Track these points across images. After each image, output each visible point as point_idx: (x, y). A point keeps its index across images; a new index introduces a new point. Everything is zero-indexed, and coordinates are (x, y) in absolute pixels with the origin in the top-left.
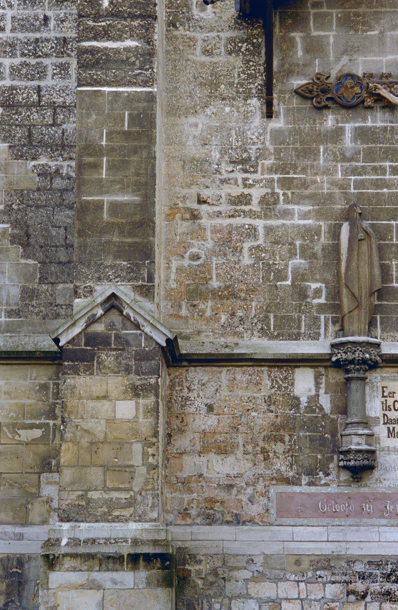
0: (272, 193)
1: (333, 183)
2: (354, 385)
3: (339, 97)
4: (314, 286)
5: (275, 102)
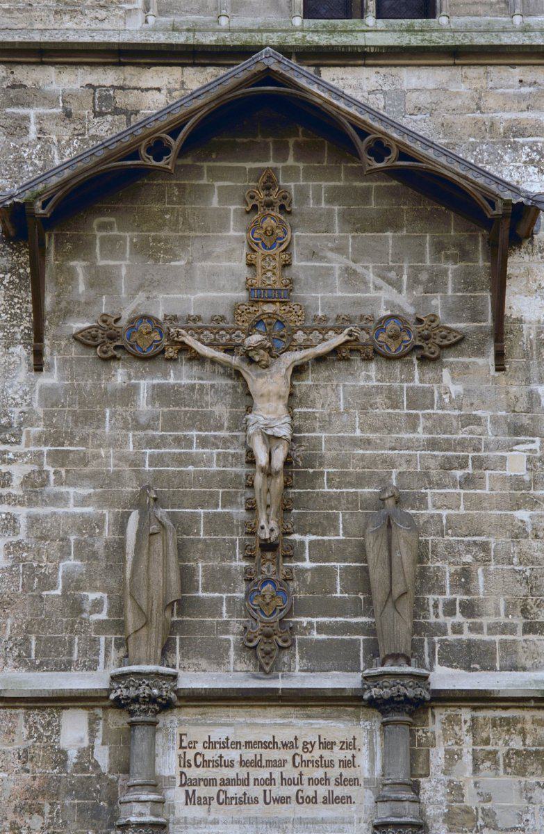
0: (39, 471)
1: (122, 458)
2: (139, 733)
3: (132, 346)
4: (93, 596)
5: (47, 350)
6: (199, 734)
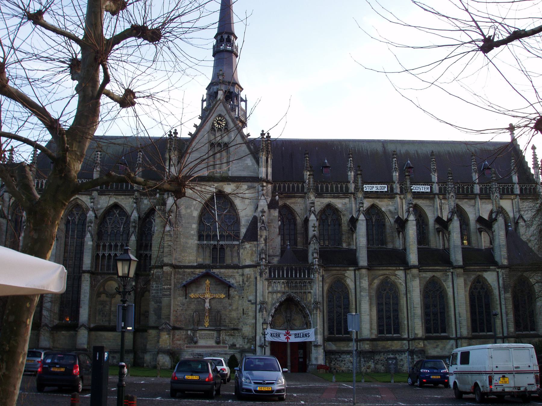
6: (200, 333)
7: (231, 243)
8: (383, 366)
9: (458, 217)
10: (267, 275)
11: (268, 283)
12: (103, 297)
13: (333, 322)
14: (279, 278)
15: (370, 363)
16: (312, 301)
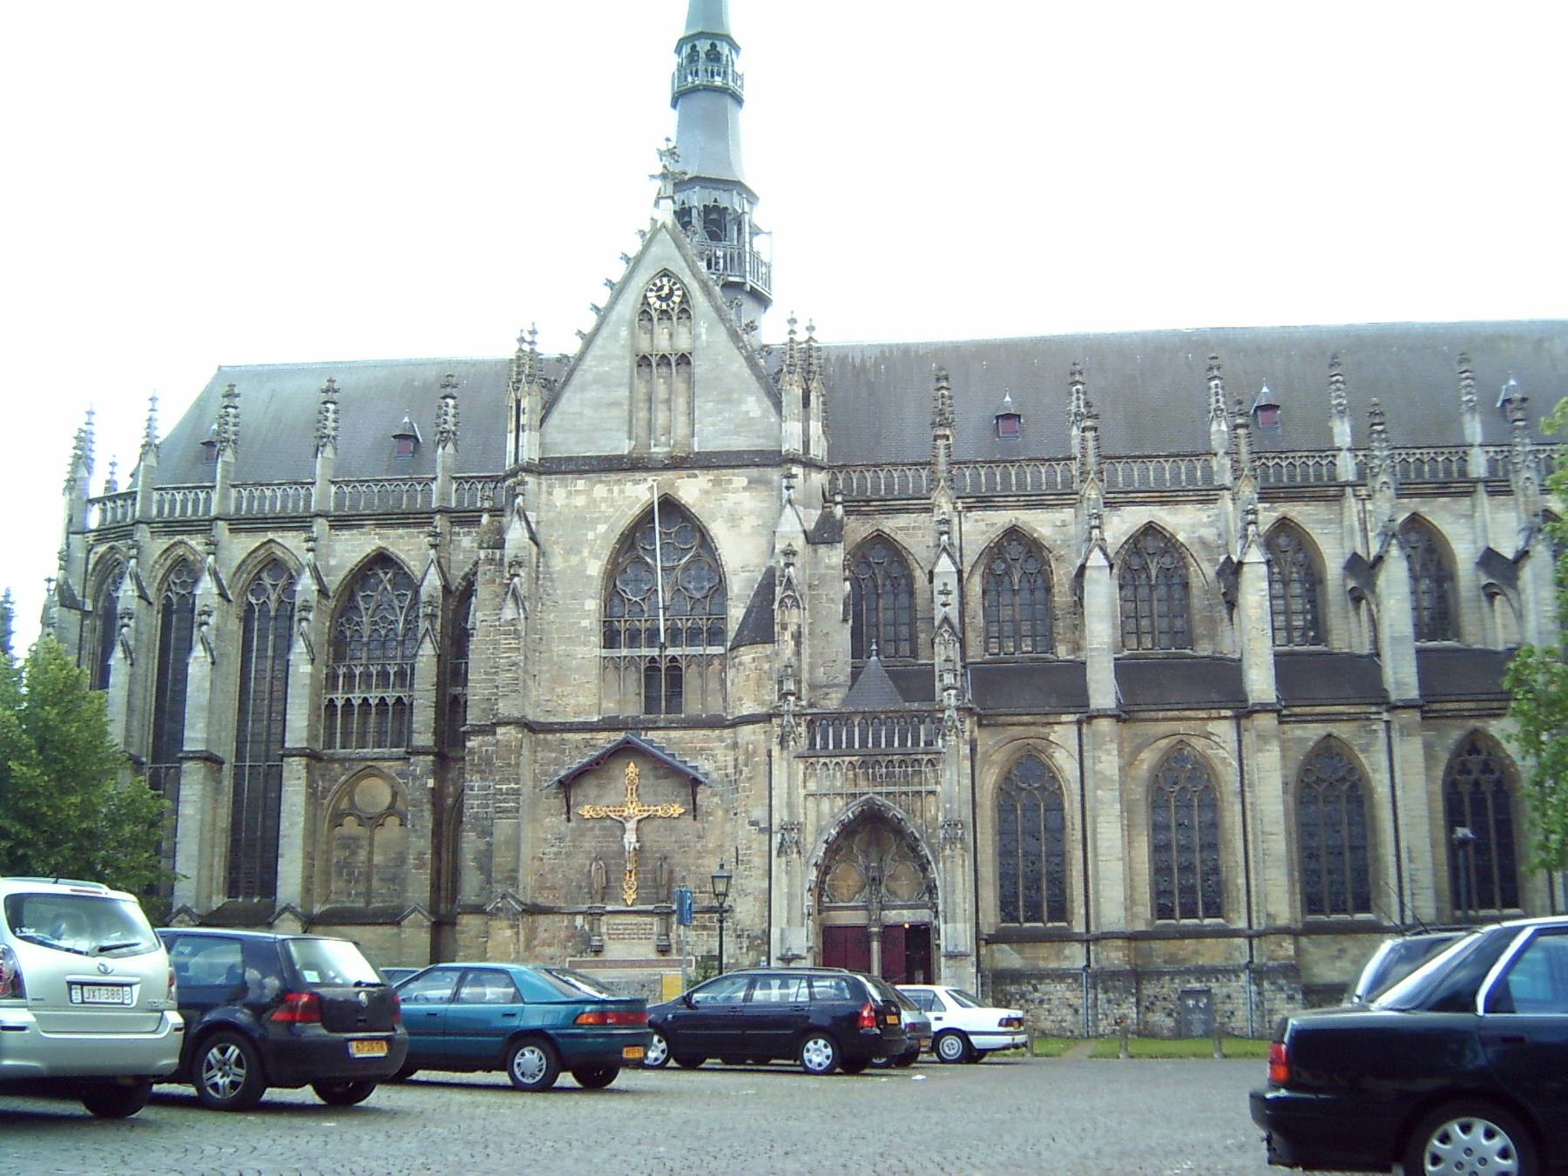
7: (699, 650)
8: (1169, 1015)
9: (1402, 548)
10: (804, 742)
11: (806, 768)
12: (350, 826)
13: (1016, 883)
14: (838, 751)
15: (1125, 1006)
16: (940, 819)
